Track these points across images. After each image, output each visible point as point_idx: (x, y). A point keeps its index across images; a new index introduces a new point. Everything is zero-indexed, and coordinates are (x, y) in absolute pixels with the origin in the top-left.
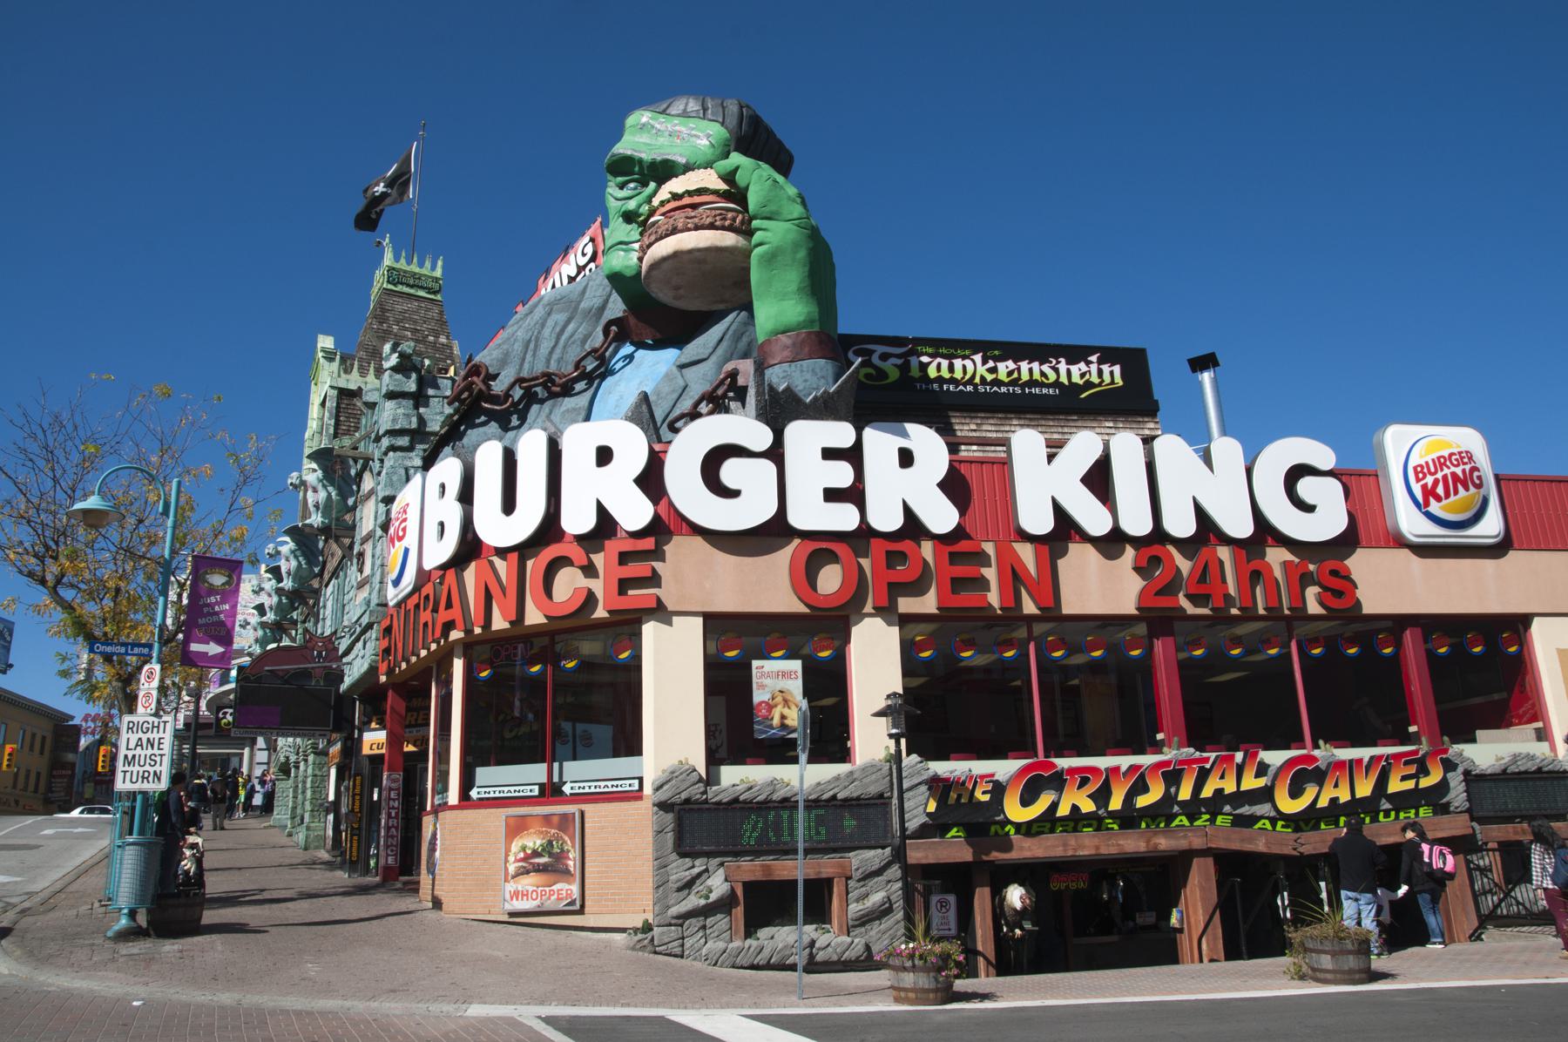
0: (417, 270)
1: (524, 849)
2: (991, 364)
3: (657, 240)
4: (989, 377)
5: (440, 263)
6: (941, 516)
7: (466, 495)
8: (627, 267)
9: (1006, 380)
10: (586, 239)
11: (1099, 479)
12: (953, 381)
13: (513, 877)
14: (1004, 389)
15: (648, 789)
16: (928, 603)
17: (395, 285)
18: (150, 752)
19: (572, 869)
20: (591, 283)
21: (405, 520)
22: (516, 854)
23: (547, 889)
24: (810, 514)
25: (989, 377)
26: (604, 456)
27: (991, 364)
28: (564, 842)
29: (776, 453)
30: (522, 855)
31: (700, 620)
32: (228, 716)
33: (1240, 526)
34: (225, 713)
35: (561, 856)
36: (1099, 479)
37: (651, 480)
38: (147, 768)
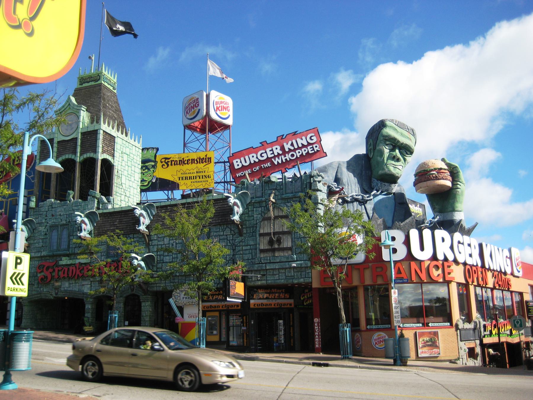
0: (110, 77)
1: (423, 340)
5: (116, 76)
10: (313, 134)
13: (421, 348)
17: (104, 82)
19: (438, 345)
22: (421, 342)
23: (431, 351)
28: (435, 338)
30: (423, 342)
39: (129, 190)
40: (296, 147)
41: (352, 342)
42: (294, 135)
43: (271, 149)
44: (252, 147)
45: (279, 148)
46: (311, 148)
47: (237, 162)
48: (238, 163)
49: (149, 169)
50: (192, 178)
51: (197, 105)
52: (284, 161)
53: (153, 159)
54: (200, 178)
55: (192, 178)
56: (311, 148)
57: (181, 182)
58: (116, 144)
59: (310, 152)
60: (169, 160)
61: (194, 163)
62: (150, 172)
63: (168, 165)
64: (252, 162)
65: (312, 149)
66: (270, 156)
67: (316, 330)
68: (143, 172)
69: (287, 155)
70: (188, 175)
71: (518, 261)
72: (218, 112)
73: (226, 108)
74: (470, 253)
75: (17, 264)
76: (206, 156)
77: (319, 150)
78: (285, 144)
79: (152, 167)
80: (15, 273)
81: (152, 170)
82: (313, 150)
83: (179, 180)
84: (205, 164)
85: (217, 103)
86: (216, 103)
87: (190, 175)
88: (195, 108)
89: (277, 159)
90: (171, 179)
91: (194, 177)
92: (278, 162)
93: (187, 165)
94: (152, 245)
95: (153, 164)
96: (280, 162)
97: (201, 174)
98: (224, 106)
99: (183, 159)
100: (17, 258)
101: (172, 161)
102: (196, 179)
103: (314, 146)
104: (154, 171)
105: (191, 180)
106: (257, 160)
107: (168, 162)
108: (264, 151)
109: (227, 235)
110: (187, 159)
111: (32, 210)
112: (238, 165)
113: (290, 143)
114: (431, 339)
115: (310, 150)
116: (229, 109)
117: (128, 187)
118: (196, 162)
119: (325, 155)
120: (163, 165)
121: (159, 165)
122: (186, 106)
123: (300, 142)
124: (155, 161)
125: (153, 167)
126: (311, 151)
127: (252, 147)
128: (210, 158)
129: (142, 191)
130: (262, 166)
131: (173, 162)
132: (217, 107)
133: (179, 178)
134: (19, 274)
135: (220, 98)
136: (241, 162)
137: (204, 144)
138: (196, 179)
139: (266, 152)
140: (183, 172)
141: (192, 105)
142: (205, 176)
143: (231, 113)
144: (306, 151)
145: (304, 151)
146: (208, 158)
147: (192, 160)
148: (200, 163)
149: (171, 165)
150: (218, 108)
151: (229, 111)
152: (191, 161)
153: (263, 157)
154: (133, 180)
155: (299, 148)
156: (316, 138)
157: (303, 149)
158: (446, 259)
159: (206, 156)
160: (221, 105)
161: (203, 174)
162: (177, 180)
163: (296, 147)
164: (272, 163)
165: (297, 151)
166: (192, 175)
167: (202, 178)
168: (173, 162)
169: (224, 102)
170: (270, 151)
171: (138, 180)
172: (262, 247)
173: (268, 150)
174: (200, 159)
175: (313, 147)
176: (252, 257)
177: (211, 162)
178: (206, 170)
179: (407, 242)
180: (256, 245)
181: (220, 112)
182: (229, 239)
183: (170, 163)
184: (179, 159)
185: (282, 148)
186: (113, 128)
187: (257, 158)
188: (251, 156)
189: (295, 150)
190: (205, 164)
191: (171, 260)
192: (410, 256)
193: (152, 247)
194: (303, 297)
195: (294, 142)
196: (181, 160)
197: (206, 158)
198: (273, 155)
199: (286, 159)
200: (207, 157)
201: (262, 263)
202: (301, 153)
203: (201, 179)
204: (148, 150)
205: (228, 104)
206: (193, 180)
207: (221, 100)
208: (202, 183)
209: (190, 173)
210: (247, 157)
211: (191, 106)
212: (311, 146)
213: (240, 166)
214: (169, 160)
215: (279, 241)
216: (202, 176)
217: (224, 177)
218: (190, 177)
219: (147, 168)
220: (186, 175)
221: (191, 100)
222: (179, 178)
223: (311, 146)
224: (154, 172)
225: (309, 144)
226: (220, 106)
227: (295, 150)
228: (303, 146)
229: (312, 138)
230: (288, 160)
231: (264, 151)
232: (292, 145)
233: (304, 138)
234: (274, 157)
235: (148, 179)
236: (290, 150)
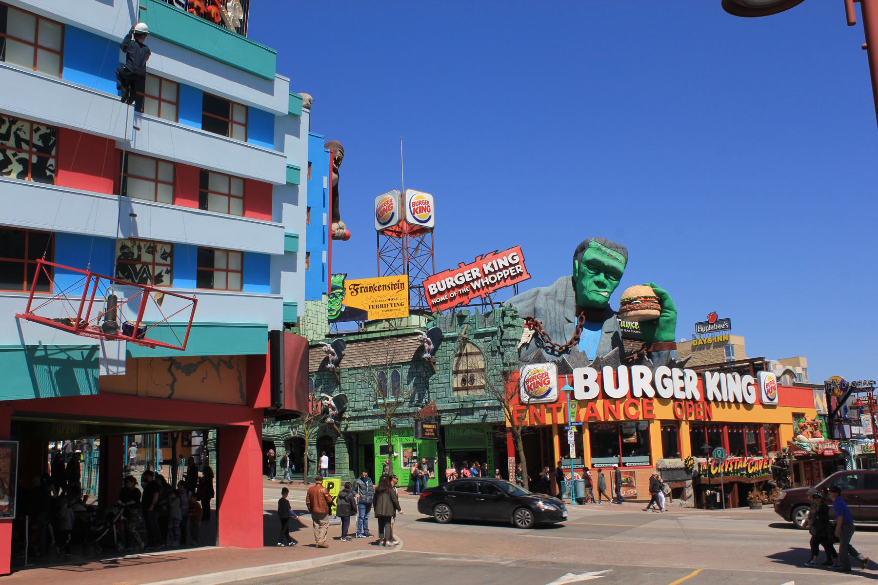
2: (633, 323)
3: (640, 309)
4: (633, 327)
6: (698, 397)
7: (601, 381)
8: (601, 301)
9: (637, 328)
10: (515, 254)
11: (719, 386)
12: (626, 328)
14: (636, 332)
15: (654, 465)
16: (692, 418)
19: (634, 485)
20: (558, 290)
24: (680, 395)
25: (633, 327)
26: (642, 375)
27: (633, 323)
28: (632, 479)
29: (671, 377)
31: (659, 422)
33: (740, 400)
35: (631, 482)
36: (719, 386)
37: (653, 384)
39: (316, 316)
42: (495, 254)
43: (469, 271)
44: (449, 269)
45: (478, 270)
46: (512, 270)
47: (432, 287)
48: (433, 289)
49: (337, 297)
50: (384, 306)
51: (390, 208)
53: (341, 286)
54: (392, 306)
55: (384, 306)
56: (512, 270)
59: (512, 274)
60: (358, 287)
61: (386, 289)
62: (338, 300)
63: (357, 292)
64: (449, 287)
65: (514, 271)
66: (468, 280)
67: (511, 471)
68: (331, 300)
70: (379, 303)
71: (769, 388)
72: (416, 215)
73: (426, 209)
74: (683, 386)
76: (398, 281)
77: (522, 271)
78: (484, 266)
79: (340, 294)
81: (340, 297)
82: (516, 271)
83: (370, 308)
84: (397, 290)
85: (414, 204)
86: (413, 204)
87: (381, 303)
91: (385, 305)
92: (477, 286)
93: (377, 291)
94: (343, 383)
96: (479, 287)
97: (393, 302)
98: (422, 206)
99: (374, 285)
101: (361, 288)
102: (387, 307)
103: (517, 267)
104: (342, 298)
105: (382, 309)
106: (454, 285)
107: (358, 288)
108: (461, 274)
109: (420, 372)
110: (379, 285)
112: (434, 291)
113: (490, 264)
114: (627, 479)
116: (430, 209)
117: (314, 312)
118: (387, 288)
119: (529, 277)
120: (353, 292)
121: (348, 292)
122: (378, 207)
123: (501, 262)
124: (343, 288)
125: (341, 294)
126: (513, 272)
127: (449, 269)
129: (330, 321)
130: (460, 291)
131: (363, 289)
132: (414, 209)
133: (370, 306)
135: (418, 198)
136: (437, 287)
137: (402, 251)
138: (387, 307)
139: (464, 276)
140: (374, 300)
141: (385, 207)
142: (397, 303)
143: (432, 213)
145: (505, 273)
146: (401, 284)
147: (383, 285)
148: (392, 289)
149: (361, 292)
150: (415, 210)
151: (429, 212)
152: (382, 287)
153: (461, 281)
154: (320, 304)
155: (500, 270)
156: (519, 257)
157: (504, 271)
158: (644, 395)
159: (398, 281)
160: (419, 206)
161: (396, 302)
162: (366, 308)
163: (497, 269)
165: (498, 274)
166: (383, 303)
167: (395, 306)
168: (363, 289)
170: (468, 274)
171: (326, 303)
172: (455, 386)
173: (466, 273)
174: (392, 285)
175: (515, 269)
176: (446, 396)
177: (404, 287)
178: (399, 297)
179: (601, 381)
180: (449, 383)
182: (422, 376)
183: (359, 290)
184: (369, 285)
187: (454, 282)
188: (447, 280)
189: (495, 272)
190: (397, 290)
191: (364, 399)
192: (603, 395)
193: (343, 384)
195: (494, 263)
196: (372, 287)
197: (398, 284)
198: (471, 279)
199: (486, 283)
200: (400, 282)
201: (456, 402)
202: (502, 276)
203: (393, 308)
204: (335, 276)
205: (428, 203)
206: (384, 309)
207: (418, 200)
208: (394, 312)
210: (443, 281)
211: (384, 208)
212: (514, 267)
213: (436, 291)
214: (358, 287)
215: (472, 380)
216: (395, 304)
217: (419, 302)
218: (381, 305)
220: (377, 303)
221: (383, 201)
222: (370, 306)
223: (514, 267)
224: (342, 300)
225: (511, 265)
226: (417, 208)
227: (495, 272)
228: (505, 267)
229: (514, 258)
230: (488, 283)
231: (461, 274)
232: (492, 266)
233: (505, 258)
234: (473, 281)
235: (336, 307)
236: (490, 273)
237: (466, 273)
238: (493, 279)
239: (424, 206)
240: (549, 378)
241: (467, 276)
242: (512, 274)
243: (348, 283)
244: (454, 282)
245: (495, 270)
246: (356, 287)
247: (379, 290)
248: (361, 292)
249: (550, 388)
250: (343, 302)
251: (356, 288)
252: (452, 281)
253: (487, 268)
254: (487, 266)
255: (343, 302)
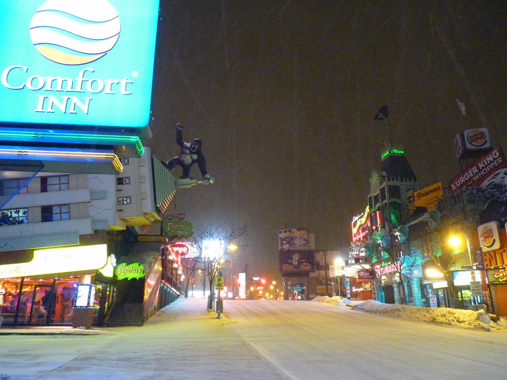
18: (477, 288)
21: (492, 233)
32: (361, 274)
34: (361, 273)
38: (477, 291)
40: (486, 164)
41: (210, 302)
43: (471, 170)
45: (476, 168)
46: (496, 162)
52: (480, 177)
56: (496, 162)
57: (428, 206)
58: (401, 190)
59: (496, 165)
62: (413, 204)
63: (420, 197)
64: (462, 183)
65: (497, 162)
66: (471, 176)
69: (481, 172)
70: (430, 201)
72: (473, 143)
75: (219, 281)
78: (479, 164)
80: (218, 284)
82: (498, 163)
85: (470, 137)
88: (458, 146)
89: (476, 176)
90: (422, 205)
92: (477, 179)
93: (429, 195)
95: (413, 198)
96: (478, 178)
98: (478, 137)
100: (219, 279)
101: (421, 194)
103: (498, 159)
106: (464, 181)
107: (420, 195)
108: (467, 173)
111: (202, 268)
115: (495, 163)
121: (416, 198)
124: (414, 197)
126: (497, 164)
128: (440, 187)
130: (468, 184)
134: (220, 284)
139: (469, 174)
144: (493, 165)
146: (439, 187)
147: (431, 190)
149: (422, 197)
155: (488, 164)
157: (491, 165)
159: (437, 186)
160: (474, 137)
162: (426, 206)
164: (474, 181)
168: (422, 195)
169: (477, 134)
175: (497, 161)
177: (440, 189)
181: (475, 142)
183: (421, 196)
185: (478, 168)
186: (397, 180)
187: (464, 179)
188: (460, 179)
189: (486, 166)
194: (498, 276)
195: (485, 160)
197: (438, 188)
199: (481, 175)
200: (438, 186)
209: (431, 199)
210: (458, 181)
212: (496, 160)
219: (411, 202)
223: (496, 160)
225: (494, 159)
227: (486, 166)
228: (491, 162)
230: (483, 175)
232: (484, 163)
233: (490, 156)
234: (474, 176)
237: (470, 172)
238: (485, 171)
239: (479, 136)
240: (492, 233)
241: (470, 173)
242: (496, 165)
243: (415, 194)
244: (464, 179)
245: (485, 165)
246: (419, 195)
247: (429, 194)
248: (422, 197)
249: (494, 239)
250: (415, 205)
251: (420, 196)
252: (463, 178)
253: (481, 166)
254: (481, 164)
255: (415, 205)
